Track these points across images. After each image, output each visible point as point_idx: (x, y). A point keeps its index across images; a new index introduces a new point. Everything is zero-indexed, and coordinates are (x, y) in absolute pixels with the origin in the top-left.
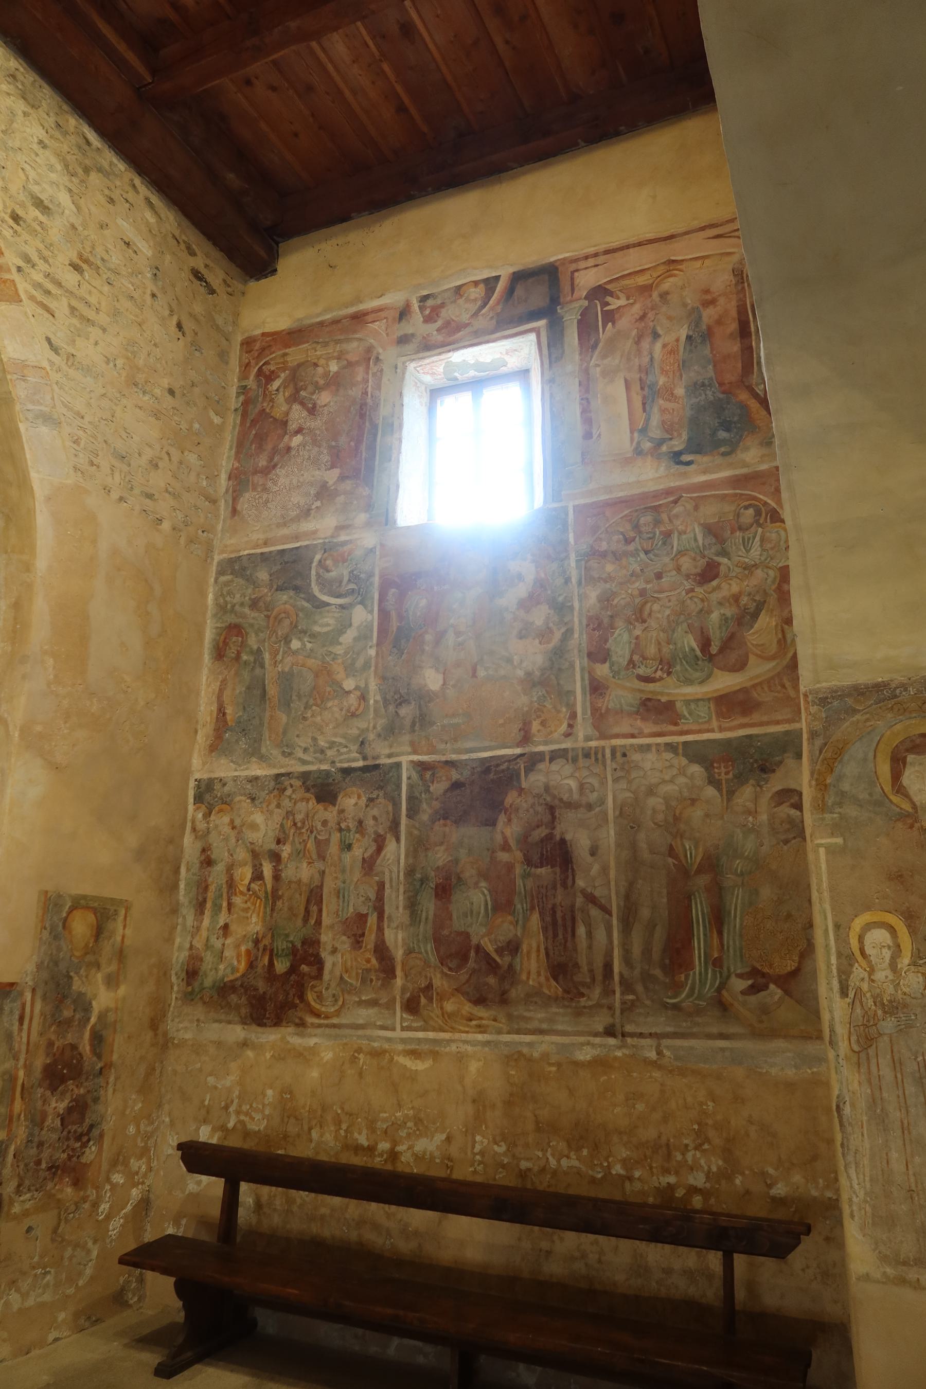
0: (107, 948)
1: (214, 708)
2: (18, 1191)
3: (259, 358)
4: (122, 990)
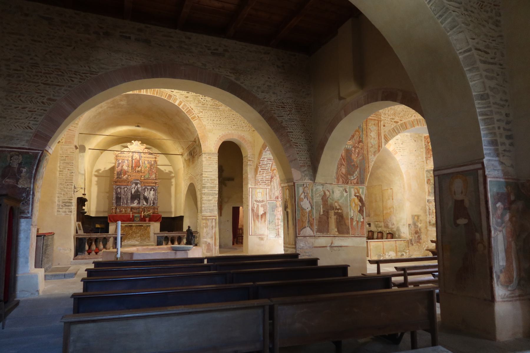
0: (419, 220)
1: (428, 190)
2: (414, 243)
3: (427, 139)
4: (422, 224)
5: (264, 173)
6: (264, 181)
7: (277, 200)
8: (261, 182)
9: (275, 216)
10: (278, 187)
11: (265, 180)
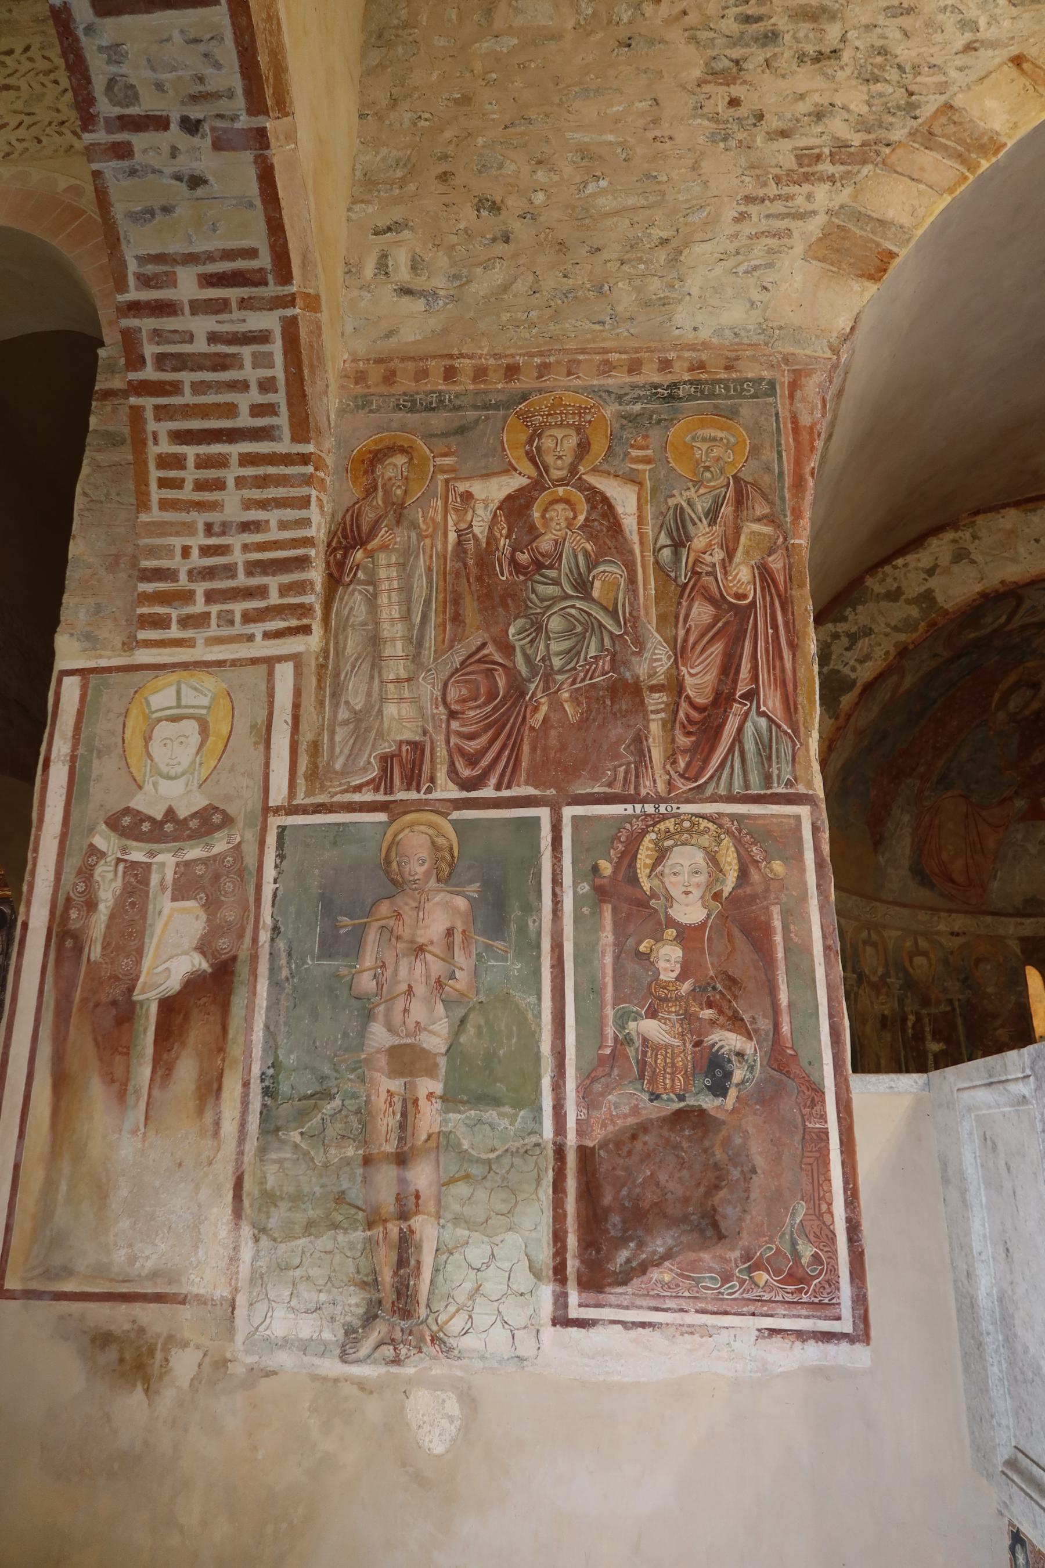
5: (219, 485)
6: (242, 580)
7: (401, 795)
8: (200, 588)
9: (368, 1016)
10: (431, 633)
11: (252, 568)
